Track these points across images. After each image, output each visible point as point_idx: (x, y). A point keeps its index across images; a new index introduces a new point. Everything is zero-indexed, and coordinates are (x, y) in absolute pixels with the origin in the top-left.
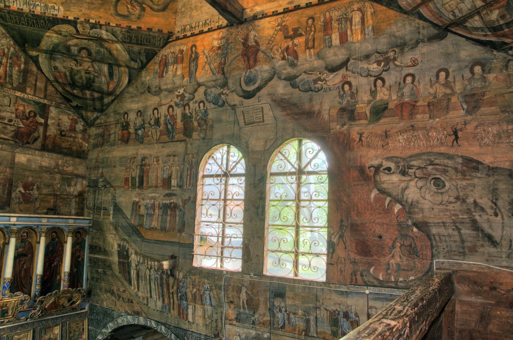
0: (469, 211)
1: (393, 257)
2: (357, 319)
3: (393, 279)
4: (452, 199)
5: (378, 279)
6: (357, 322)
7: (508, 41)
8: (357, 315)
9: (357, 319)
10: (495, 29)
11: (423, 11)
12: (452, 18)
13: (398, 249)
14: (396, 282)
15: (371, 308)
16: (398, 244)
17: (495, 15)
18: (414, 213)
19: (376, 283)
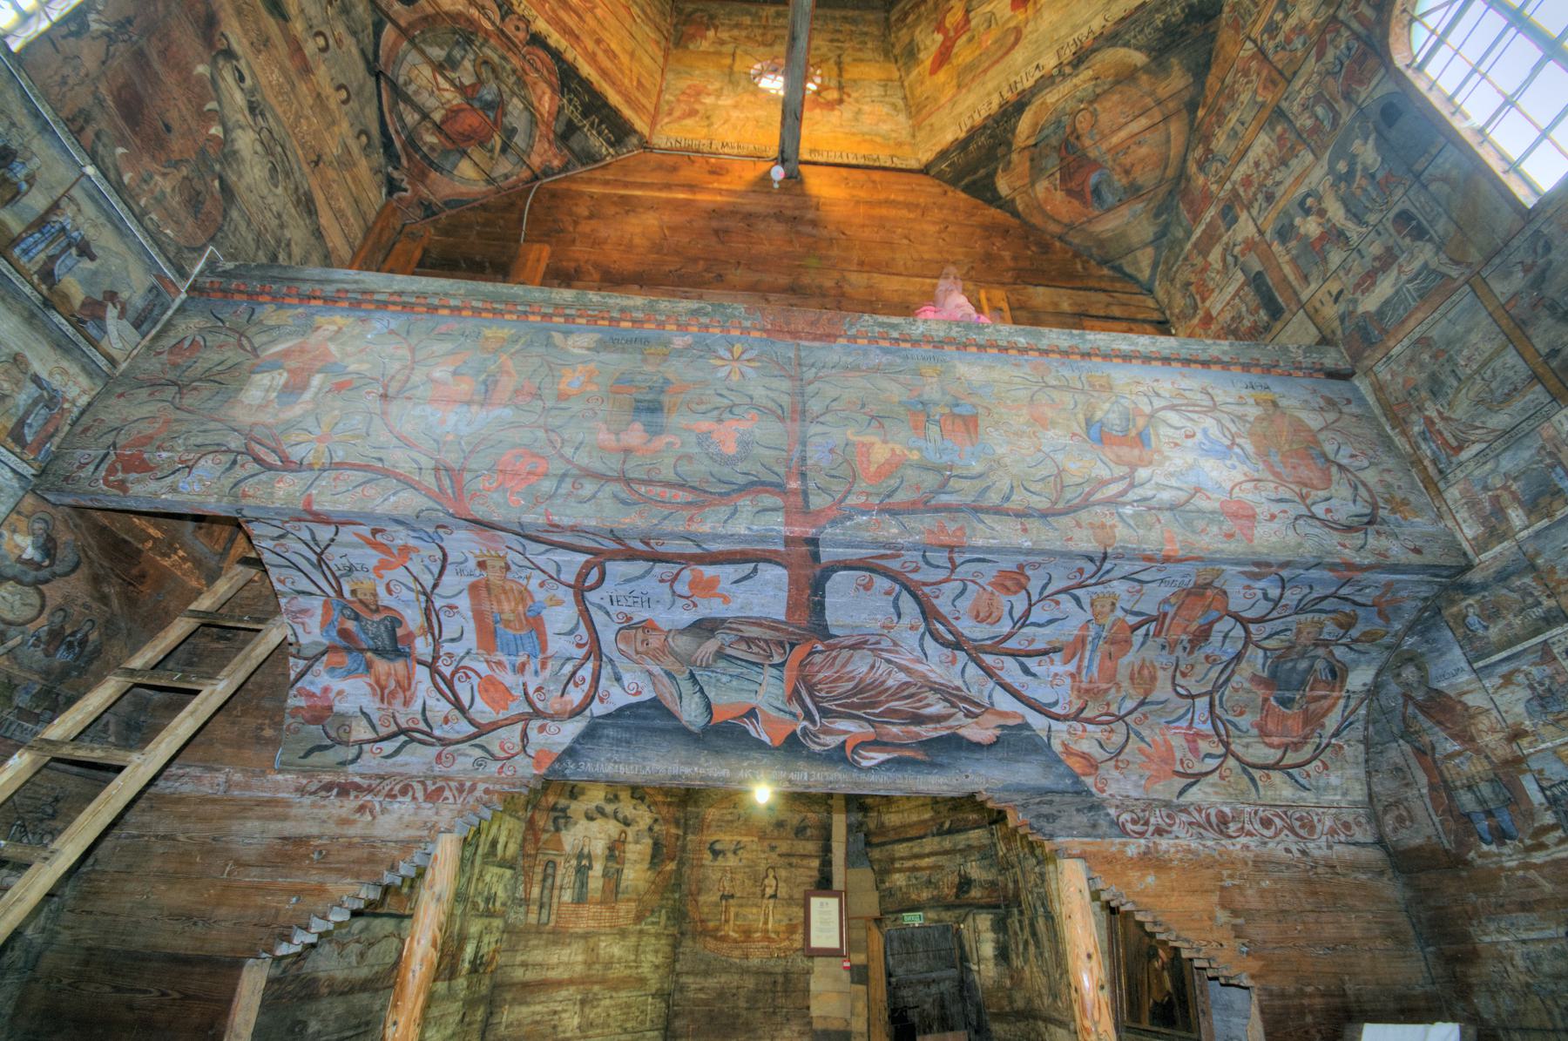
0: (278, 241)
1: (164, 175)
2: (25, 187)
3: (142, 203)
4: (274, 209)
5: (120, 176)
6: (18, 193)
7: (404, 161)
8: (31, 179)
9: (25, 187)
10: (412, 143)
11: (389, 32)
12: (401, 80)
13: (179, 176)
14: (145, 212)
15: (71, 199)
16: (185, 171)
17: (431, 139)
18: (230, 164)
19: (112, 175)
